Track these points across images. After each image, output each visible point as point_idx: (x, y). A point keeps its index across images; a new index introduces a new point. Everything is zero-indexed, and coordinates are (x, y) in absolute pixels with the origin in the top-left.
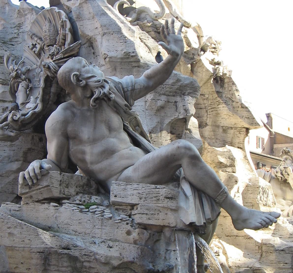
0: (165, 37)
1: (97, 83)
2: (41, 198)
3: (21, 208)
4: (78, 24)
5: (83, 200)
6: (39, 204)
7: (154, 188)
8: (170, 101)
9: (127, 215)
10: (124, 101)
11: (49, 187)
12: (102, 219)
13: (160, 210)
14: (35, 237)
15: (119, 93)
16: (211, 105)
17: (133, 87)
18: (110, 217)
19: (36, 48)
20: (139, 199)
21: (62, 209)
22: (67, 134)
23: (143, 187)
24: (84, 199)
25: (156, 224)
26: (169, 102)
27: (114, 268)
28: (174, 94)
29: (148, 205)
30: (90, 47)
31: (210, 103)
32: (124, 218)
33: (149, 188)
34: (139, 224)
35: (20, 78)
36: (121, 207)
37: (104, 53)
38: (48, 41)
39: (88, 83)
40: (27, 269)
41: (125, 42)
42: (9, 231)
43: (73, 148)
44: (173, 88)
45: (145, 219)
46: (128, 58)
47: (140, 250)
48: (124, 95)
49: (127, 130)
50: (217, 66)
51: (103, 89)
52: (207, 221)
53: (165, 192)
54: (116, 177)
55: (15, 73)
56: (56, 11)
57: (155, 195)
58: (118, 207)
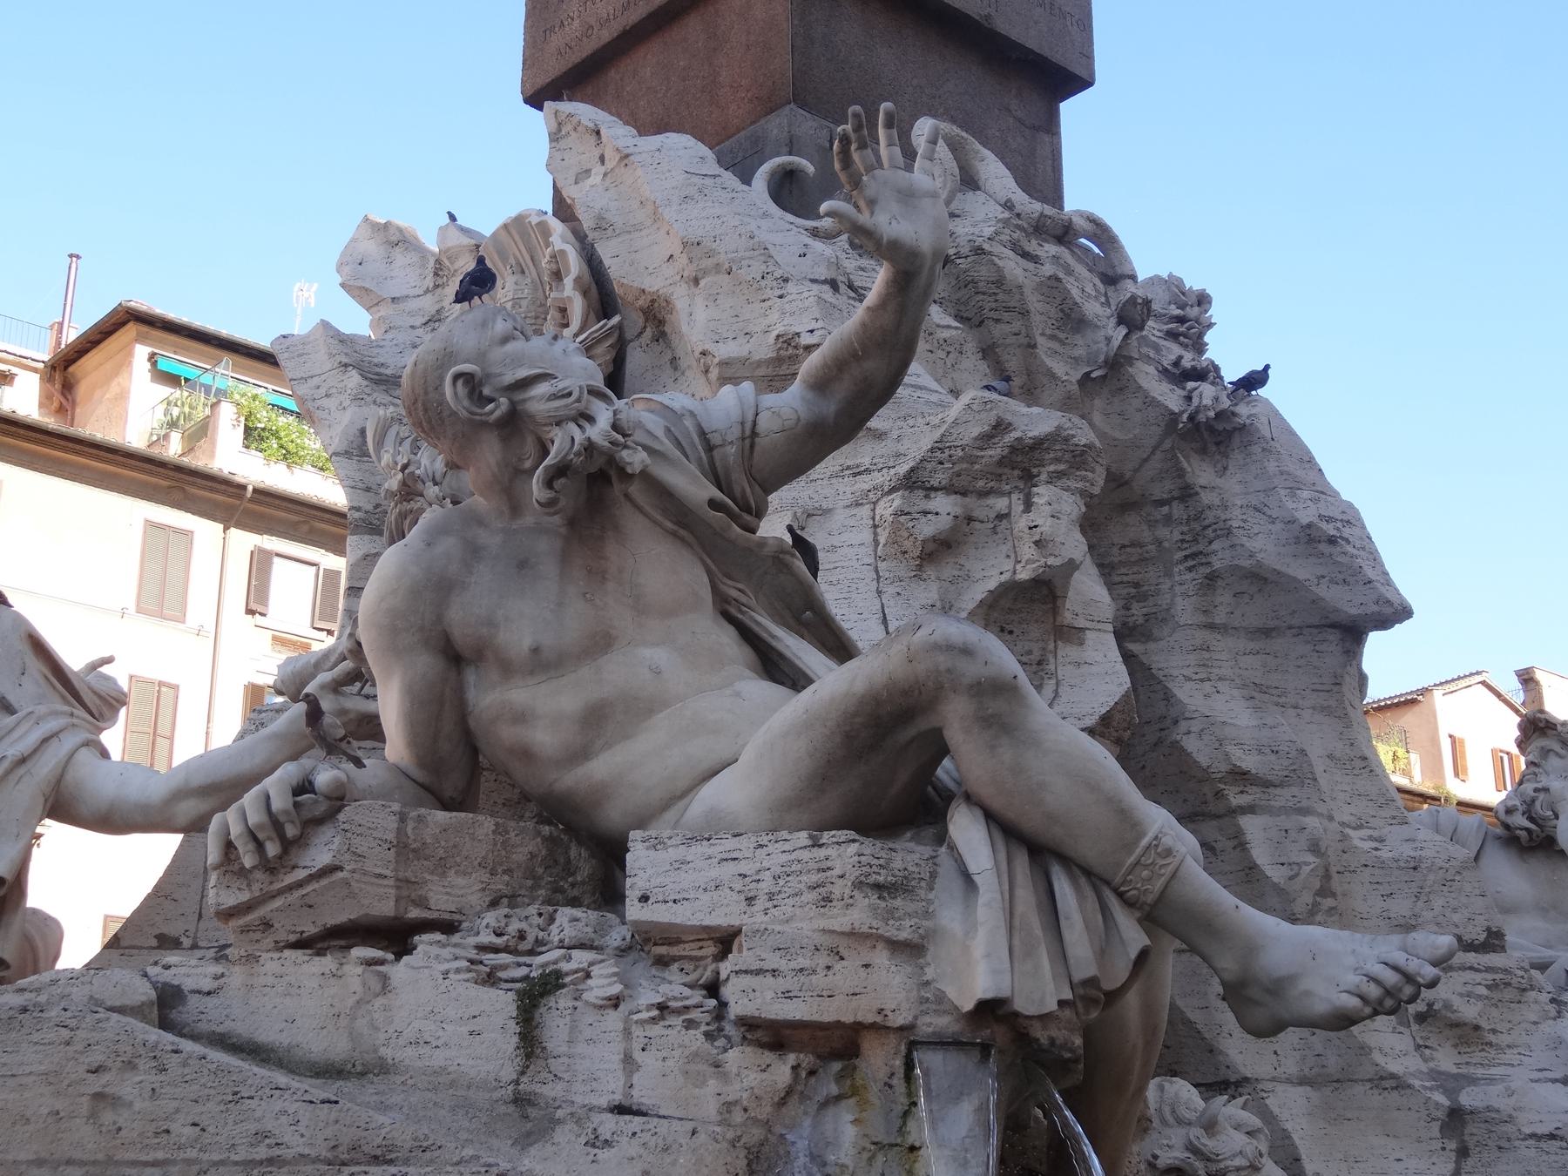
0: (856, 183)
2: (311, 930)
4: (607, 252)
5: (514, 926)
7: (805, 847)
8: (975, 514)
9: (701, 982)
11: (340, 875)
13: (841, 949)
15: (687, 457)
16: (1185, 545)
17: (748, 426)
18: (609, 999)
21: (400, 971)
23: (761, 846)
24: (523, 925)
25: (820, 1019)
26: (970, 519)
28: (992, 483)
30: (657, 341)
31: (1181, 537)
32: (675, 999)
33: (787, 846)
34: (750, 1025)
35: (422, 495)
37: (700, 350)
39: (519, 408)
41: (781, 297)
42: (96, 1084)
44: (983, 461)
45: (769, 995)
47: (743, 1153)
49: (740, 616)
50: (1191, 385)
51: (587, 425)
52: (1081, 991)
53: (856, 858)
54: (670, 815)
55: (400, 476)
56: (530, 222)
57: (815, 878)
58: (662, 950)
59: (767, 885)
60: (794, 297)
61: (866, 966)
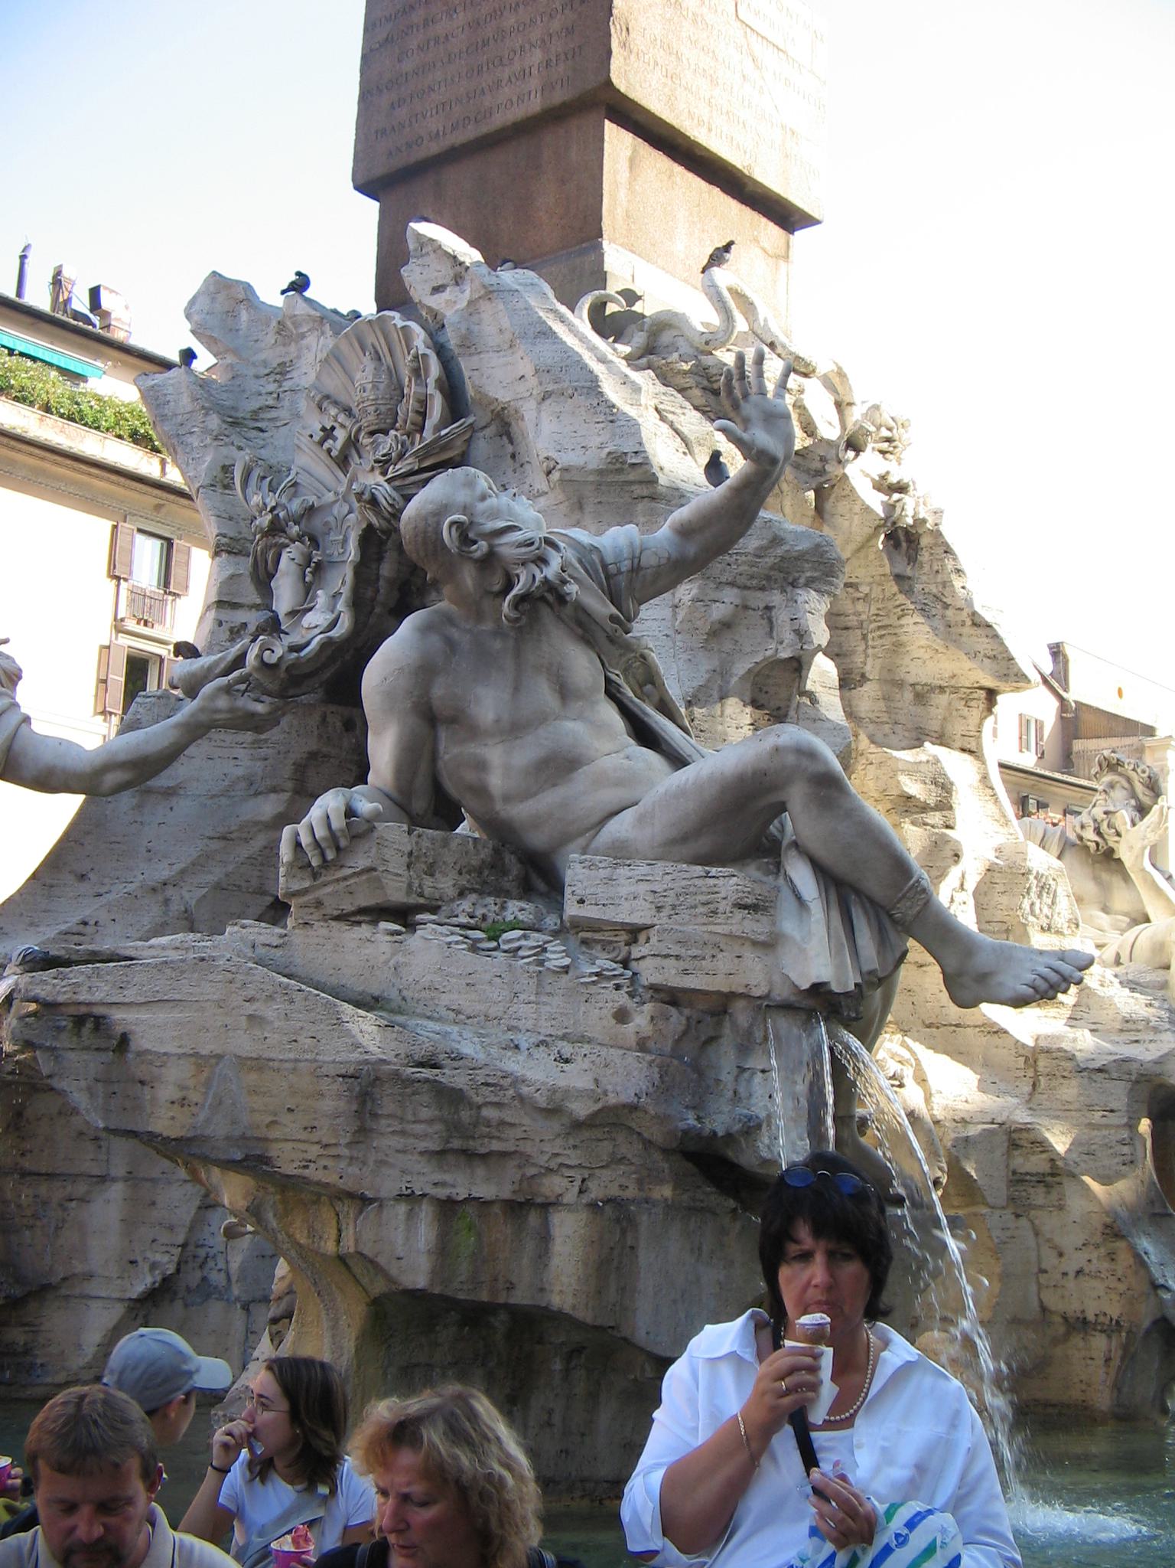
0: (736, 406)
1: (523, 550)
2: (348, 907)
3: (286, 938)
4: (465, 365)
5: (479, 912)
6: (342, 926)
8: (749, 603)
9: (619, 959)
10: (607, 606)
11: (375, 873)
12: (540, 972)
14: (330, 1028)
16: (879, 618)
17: (636, 561)
18: (563, 967)
19: (335, 439)
20: (653, 912)
21: (415, 941)
22: (431, 709)
24: (484, 911)
26: (746, 607)
27: (578, 1125)
29: (682, 929)
32: (608, 970)
34: (655, 988)
35: (285, 532)
36: (598, 936)
38: (370, 418)
39: (497, 549)
40: (306, 1128)
41: (612, 422)
42: (250, 1009)
43: (450, 750)
45: (674, 972)
46: (619, 471)
47: (657, 1070)
48: (609, 585)
50: (896, 496)
51: (543, 566)
52: (866, 978)
54: (581, 841)
55: (269, 517)
56: (395, 325)
57: (704, 898)
58: (588, 935)
59: (670, 901)
60: (622, 423)
61: (739, 957)
